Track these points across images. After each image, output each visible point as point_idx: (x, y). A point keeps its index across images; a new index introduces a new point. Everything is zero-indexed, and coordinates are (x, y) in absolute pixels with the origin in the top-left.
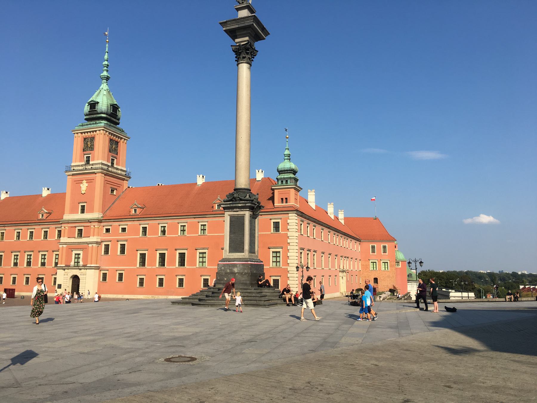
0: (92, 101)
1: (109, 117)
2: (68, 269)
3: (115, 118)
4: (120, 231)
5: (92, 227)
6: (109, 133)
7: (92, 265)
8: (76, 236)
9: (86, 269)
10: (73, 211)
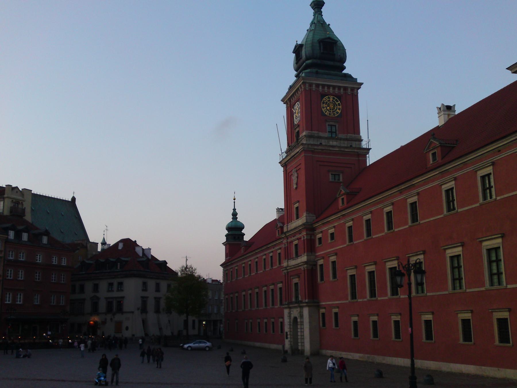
0: (296, 47)
1: (319, 61)
2: (290, 308)
4: (330, 241)
5: (302, 239)
6: (318, 85)
7: (307, 301)
8: (294, 256)
9: (301, 307)
10: (290, 220)
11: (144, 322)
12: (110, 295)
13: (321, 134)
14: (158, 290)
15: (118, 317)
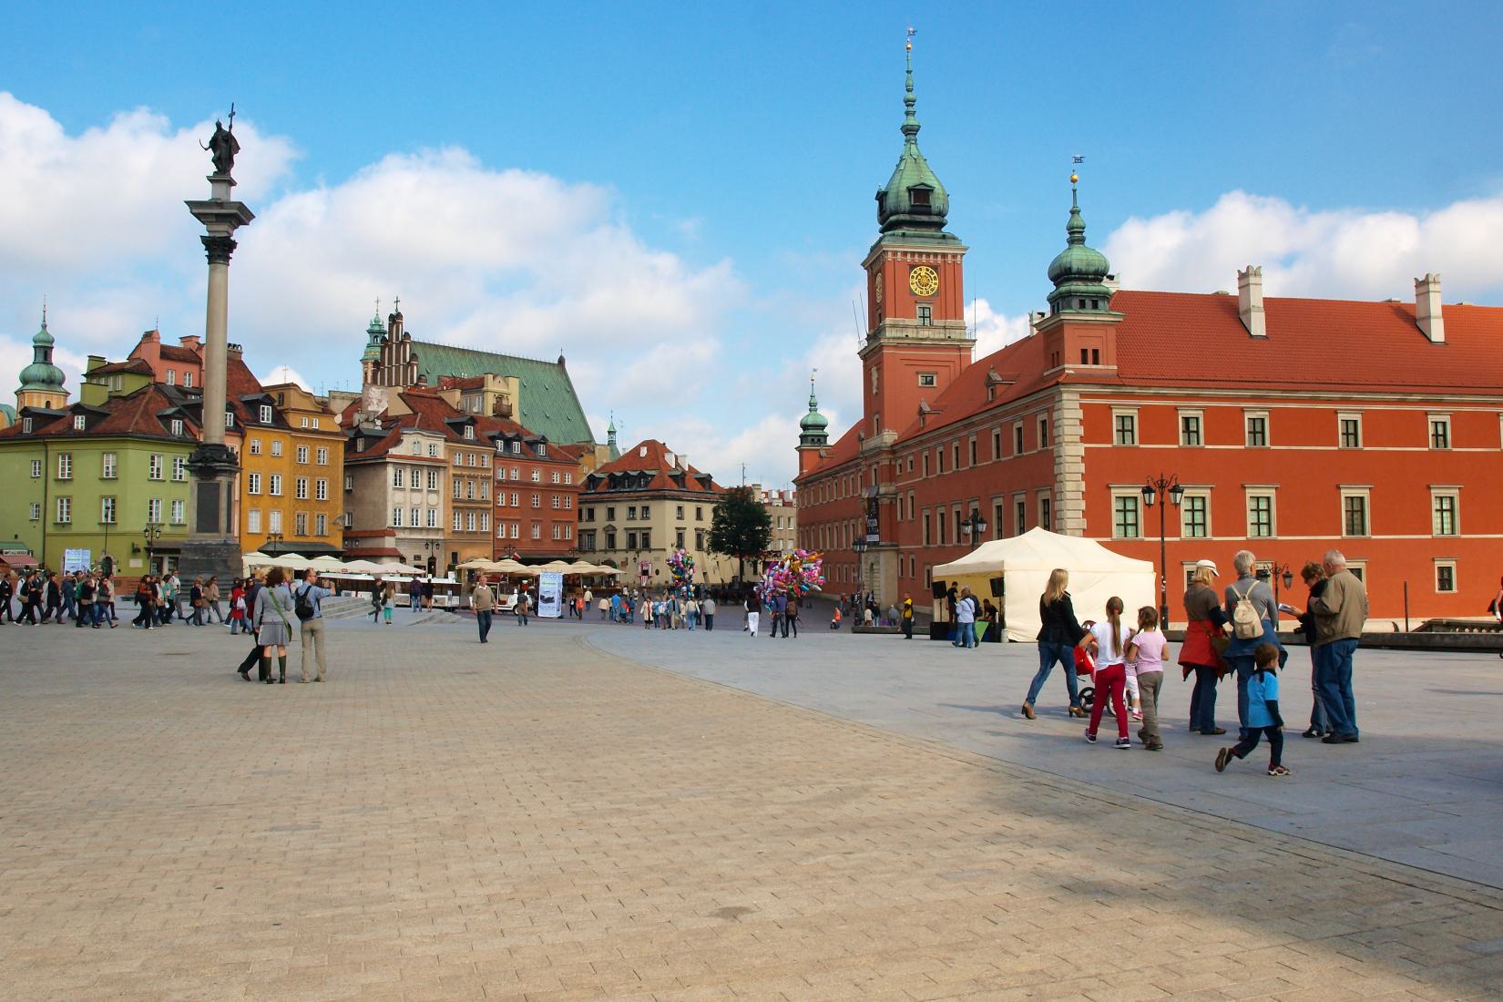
3: (929, 214)
6: (905, 254)
10: (869, 434)
13: (908, 322)
14: (699, 517)
15: (644, 556)
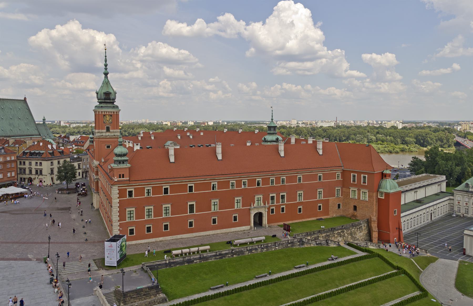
3: (110, 99)
6: (102, 112)
11: (52, 178)
12: (37, 167)
15: (40, 177)
